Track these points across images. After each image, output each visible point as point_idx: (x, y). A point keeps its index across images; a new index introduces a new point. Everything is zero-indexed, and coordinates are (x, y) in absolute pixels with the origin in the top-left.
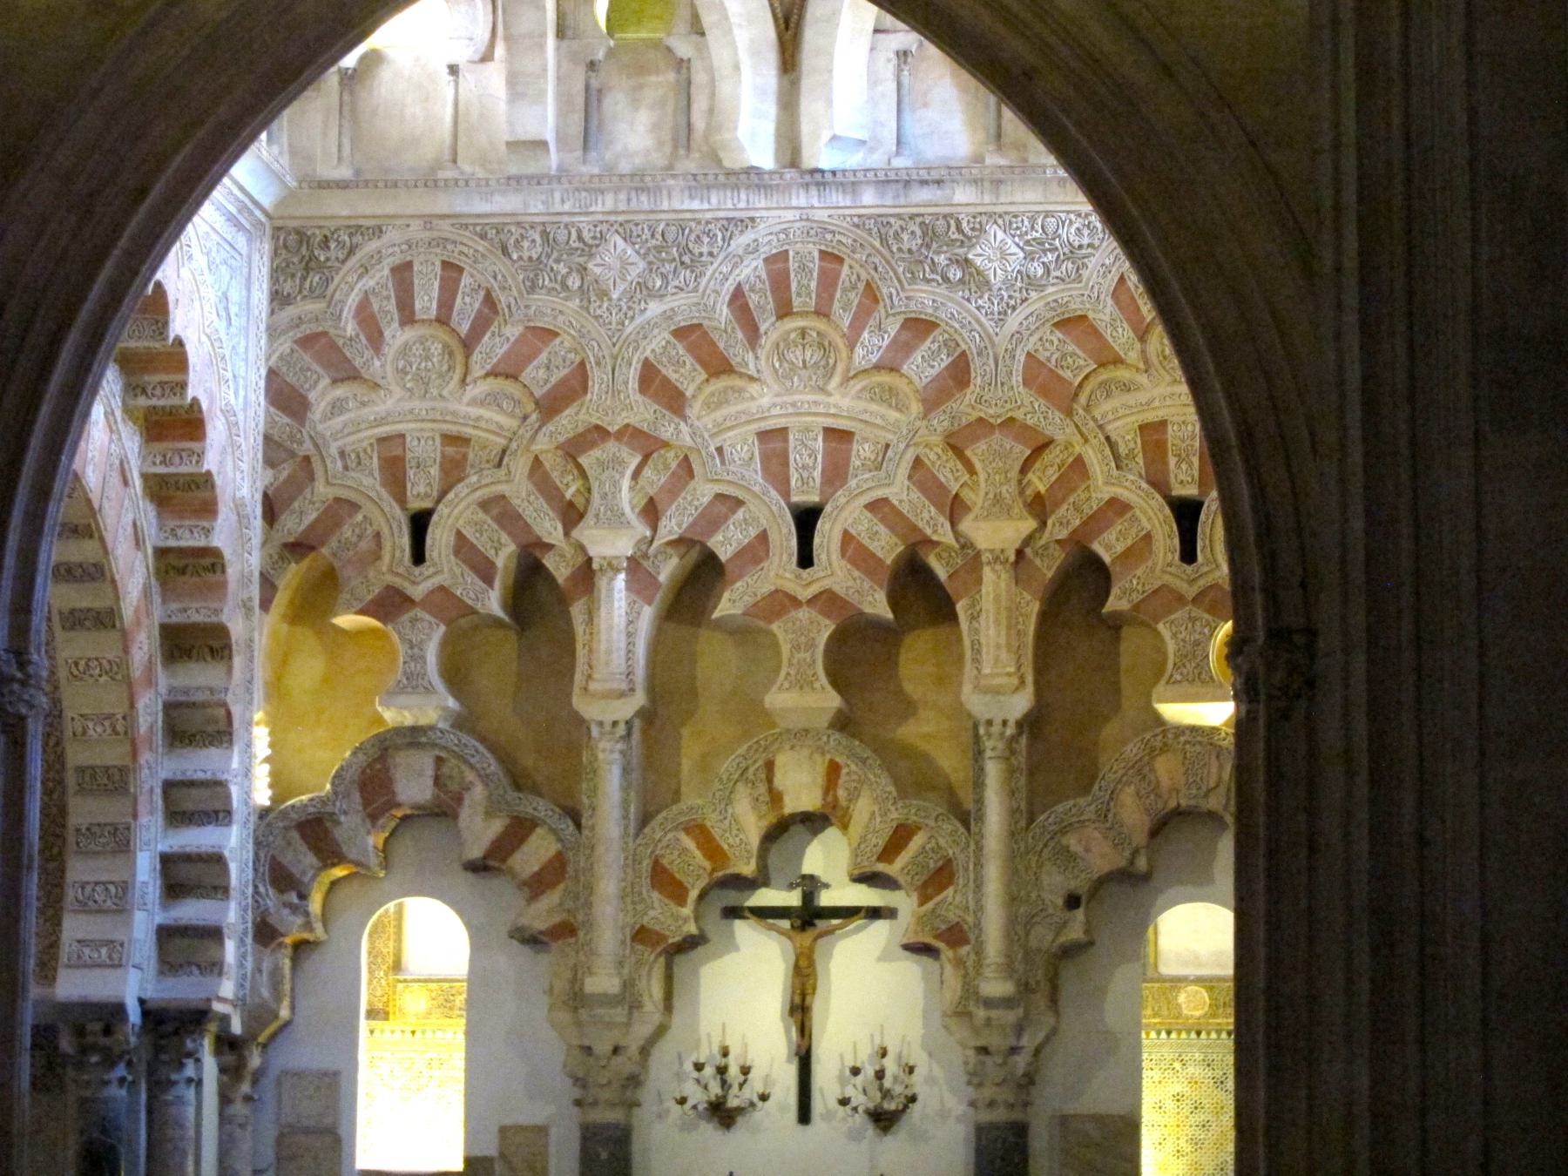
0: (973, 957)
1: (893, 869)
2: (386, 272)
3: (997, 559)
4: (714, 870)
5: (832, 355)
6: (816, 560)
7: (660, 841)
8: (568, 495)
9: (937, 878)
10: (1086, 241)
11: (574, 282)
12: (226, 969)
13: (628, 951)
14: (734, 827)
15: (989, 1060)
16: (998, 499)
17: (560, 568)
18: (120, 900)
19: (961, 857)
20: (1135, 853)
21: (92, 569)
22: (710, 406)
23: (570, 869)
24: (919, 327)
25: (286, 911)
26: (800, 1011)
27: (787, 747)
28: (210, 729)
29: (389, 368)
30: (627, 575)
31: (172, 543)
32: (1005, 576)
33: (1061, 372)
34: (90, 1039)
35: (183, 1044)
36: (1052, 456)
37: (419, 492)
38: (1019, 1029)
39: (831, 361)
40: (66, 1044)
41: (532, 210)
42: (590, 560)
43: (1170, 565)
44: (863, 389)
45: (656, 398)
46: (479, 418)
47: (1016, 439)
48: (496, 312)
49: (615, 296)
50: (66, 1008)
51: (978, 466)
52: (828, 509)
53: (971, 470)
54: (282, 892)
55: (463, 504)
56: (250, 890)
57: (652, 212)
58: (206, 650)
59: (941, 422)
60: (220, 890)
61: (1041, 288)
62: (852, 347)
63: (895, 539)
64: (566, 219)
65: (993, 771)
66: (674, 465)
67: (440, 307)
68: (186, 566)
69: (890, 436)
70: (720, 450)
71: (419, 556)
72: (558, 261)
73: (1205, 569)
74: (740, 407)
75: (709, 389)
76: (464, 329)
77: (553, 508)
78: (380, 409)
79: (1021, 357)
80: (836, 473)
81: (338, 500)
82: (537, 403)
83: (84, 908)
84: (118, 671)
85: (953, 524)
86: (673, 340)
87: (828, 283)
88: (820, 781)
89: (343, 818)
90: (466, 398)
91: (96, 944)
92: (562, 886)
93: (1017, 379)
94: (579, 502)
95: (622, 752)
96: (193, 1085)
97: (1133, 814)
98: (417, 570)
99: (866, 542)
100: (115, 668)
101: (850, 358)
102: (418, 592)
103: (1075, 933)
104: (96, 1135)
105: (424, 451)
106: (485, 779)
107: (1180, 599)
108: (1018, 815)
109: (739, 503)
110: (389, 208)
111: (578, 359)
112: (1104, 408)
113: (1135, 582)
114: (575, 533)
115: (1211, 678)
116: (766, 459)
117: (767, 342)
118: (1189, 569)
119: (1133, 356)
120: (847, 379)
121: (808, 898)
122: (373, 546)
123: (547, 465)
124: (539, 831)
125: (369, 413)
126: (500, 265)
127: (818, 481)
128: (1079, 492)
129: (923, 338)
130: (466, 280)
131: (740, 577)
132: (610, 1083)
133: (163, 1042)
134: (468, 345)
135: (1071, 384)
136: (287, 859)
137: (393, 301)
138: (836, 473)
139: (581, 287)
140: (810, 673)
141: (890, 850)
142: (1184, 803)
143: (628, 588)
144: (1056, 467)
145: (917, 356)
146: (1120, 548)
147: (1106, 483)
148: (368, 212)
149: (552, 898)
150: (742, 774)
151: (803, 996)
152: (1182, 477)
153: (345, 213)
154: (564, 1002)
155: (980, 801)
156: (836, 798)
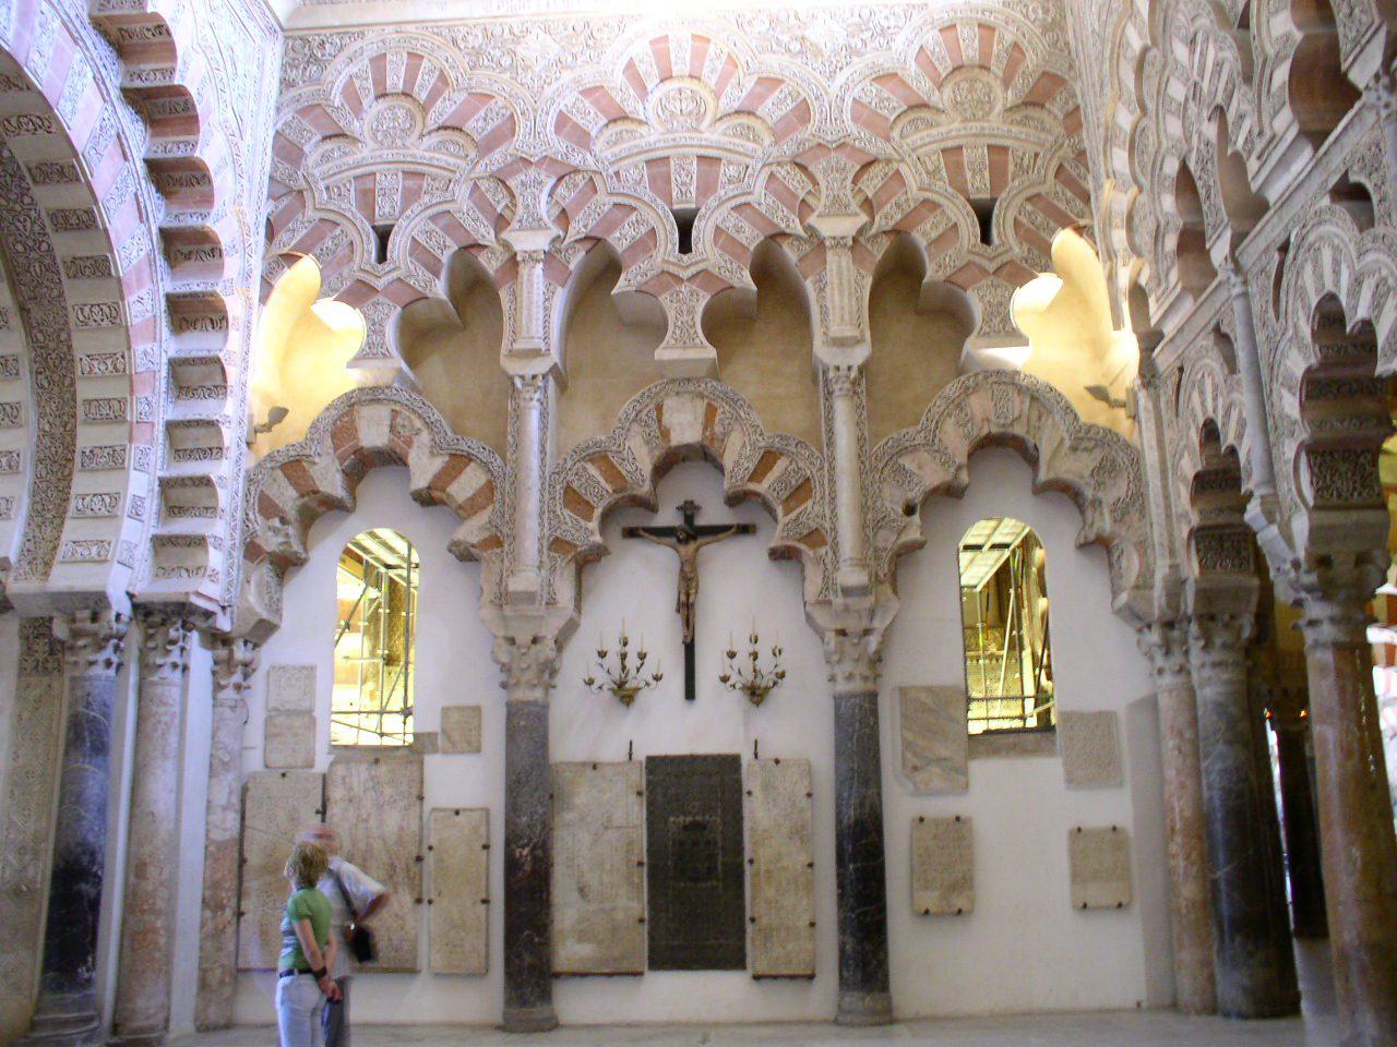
0: (830, 554)
1: (762, 487)
2: (366, 62)
8: (499, 210)
9: (800, 491)
10: (892, 24)
11: (506, 61)
12: (209, 572)
13: (545, 558)
15: (847, 641)
16: (836, 200)
17: (490, 263)
18: (109, 508)
19: (817, 475)
20: (959, 468)
21: (85, 217)
22: (610, 144)
23: (497, 495)
24: (770, 83)
25: (270, 534)
26: (686, 609)
28: (209, 384)
29: (366, 128)
30: (545, 264)
31: (174, 224)
34: (78, 625)
35: (167, 633)
36: (876, 169)
37: (384, 210)
38: (872, 613)
39: (702, 110)
40: (60, 630)
41: (476, 15)
42: (515, 254)
45: (568, 137)
46: (431, 159)
47: (848, 156)
48: (448, 85)
49: (537, 69)
50: (58, 598)
51: (819, 177)
52: (703, 210)
53: (815, 183)
54: (268, 517)
55: (418, 219)
56: (239, 515)
57: (566, 13)
58: (208, 322)
59: (788, 148)
60: (211, 510)
61: (859, 54)
62: (718, 97)
63: (756, 232)
64: (501, 20)
65: (842, 408)
66: (581, 184)
67: (405, 82)
68: (190, 253)
69: (748, 161)
70: (617, 174)
71: (382, 256)
72: (494, 48)
73: (1001, 250)
74: (633, 143)
75: (607, 133)
76: (423, 96)
77: (486, 218)
78: (359, 156)
79: (849, 101)
80: (706, 188)
81: (322, 220)
82: (476, 144)
83: (81, 515)
84: (114, 316)
85: (801, 222)
86: (580, 97)
87: (699, 56)
88: (700, 420)
89: (317, 460)
90: (422, 147)
91: (88, 543)
92: (490, 508)
93: (847, 116)
94: (507, 214)
95: (539, 400)
96: (180, 668)
97: (956, 442)
98: (380, 267)
99: (735, 235)
100: (114, 312)
101: (717, 107)
102: (380, 284)
103: (913, 534)
104: (81, 709)
105: (390, 184)
106: (429, 425)
107: (984, 272)
108: (862, 442)
110: (370, 20)
111: (509, 113)
112: (915, 138)
114: (504, 235)
116: (653, 180)
117: (653, 99)
118: (989, 249)
119: (935, 99)
121: (689, 519)
122: (347, 251)
123: (483, 189)
124: (472, 464)
125: (350, 160)
126: (453, 53)
129: (774, 90)
130: (425, 63)
131: (634, 262)
132: (529, 667)
133: (151, 631)
134: (425, 109)
135: (887, 119)
136: (272, 492)
137: (370, 80)
138: (706, 188)
139: (511, 65)
140: (692, 331)
141: (758, 474)
142: (995, 430)
143: (544, 275)
145: (769, 102)
146: (934, 235)
147: (921, 189)
148: (354, 22)
149: (482, 518)
151: (688, 595)
152: (977, 184)
153: (337, 23)
154: (492, 602)
155: (831, 432)
156: (713, 434)
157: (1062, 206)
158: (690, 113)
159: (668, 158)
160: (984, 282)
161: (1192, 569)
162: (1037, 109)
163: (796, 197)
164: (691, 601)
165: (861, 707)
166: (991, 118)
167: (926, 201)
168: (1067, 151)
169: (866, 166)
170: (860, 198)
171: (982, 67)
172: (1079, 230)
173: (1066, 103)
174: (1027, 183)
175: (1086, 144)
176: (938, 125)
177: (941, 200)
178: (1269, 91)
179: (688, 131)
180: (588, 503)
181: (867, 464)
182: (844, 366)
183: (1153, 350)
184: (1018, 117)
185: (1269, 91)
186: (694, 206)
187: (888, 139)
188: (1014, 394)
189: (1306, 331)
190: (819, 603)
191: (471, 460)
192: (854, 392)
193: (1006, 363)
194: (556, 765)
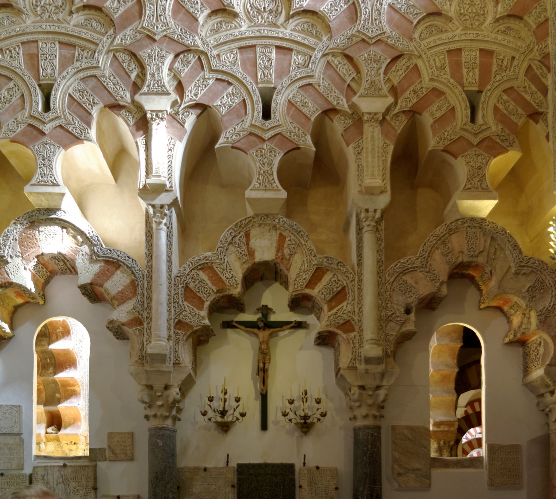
0: (357, 337)
4: (218, 291)
5: (280, 5)
6: (272, 115)
7: (188, 275)
14: (228, 268)
27: (257, 225)
33: (406, 15)
38: (382, 375)
43: (465, 124)
44: (298, 25)
52: (279, 87)
53: (358, 72)
63: (316, 107)
73: (484, 127)
85: (347, 102)
99: (301, 108)
101: (290, 7)
107: (471, 145)
109: (230, 84)
113: (446, 134)
115: (487, 186)
116: (244, 63)
120: (289, 18)
124: (121, 269)
127: (273, 76)
128: (416, 84)
144: (403, 70)
147: (432, 80)
149: (129, 306)
150: (232, 239)
152: (470, 80)
157: (528, 97)
158: (271, 11)
159: (254, 46)
160: (469, 152)
163: (345, 82)
164: (266, 367)
165: (372, 435)
167: (434, 89)
168: (536, 54)
169: (395, 59)
170: (388, 85)
173: (539, 17)
174: (505, 78)
176: (446, 31)
177: (446, 89)
179: (269, 25)
180: (200, 298)
181: (383, 279)
182: (371, 209)
186: (272, 86)
190: (349, 368)
191: (120, 266)
192: (377, 228)
194: (181, 468)
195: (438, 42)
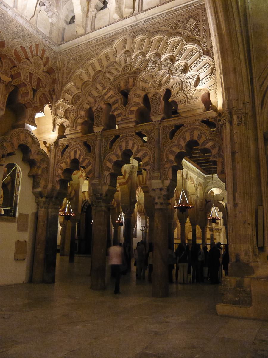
3: (4, 83)
32: (4, 87)
36: (14, 69)
51: (4, 63)
93: (13, 51)
119: (31, 60)
146: (24, 92)
161: (58, 187)
162: (48, 75)
166: (40, 70)
171: (41, 58)
172: (50, 106)
175: (55, 88)
177: (27, 85)
178: (129, 109)
183: (60, 139)
184: (44, 74)
185: (129, 109)
187: (20, 63)
188: (29, 137)
189: (120, 154)
193: (30, 129)
195: (27, 68)
